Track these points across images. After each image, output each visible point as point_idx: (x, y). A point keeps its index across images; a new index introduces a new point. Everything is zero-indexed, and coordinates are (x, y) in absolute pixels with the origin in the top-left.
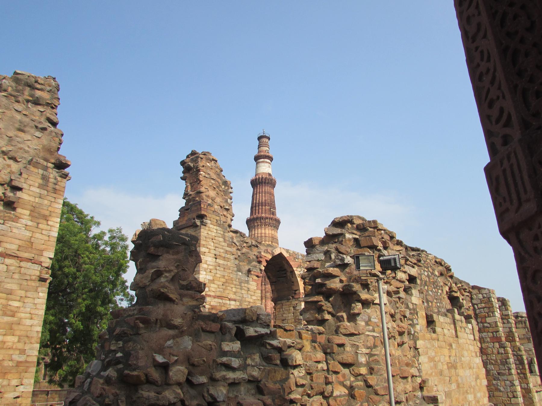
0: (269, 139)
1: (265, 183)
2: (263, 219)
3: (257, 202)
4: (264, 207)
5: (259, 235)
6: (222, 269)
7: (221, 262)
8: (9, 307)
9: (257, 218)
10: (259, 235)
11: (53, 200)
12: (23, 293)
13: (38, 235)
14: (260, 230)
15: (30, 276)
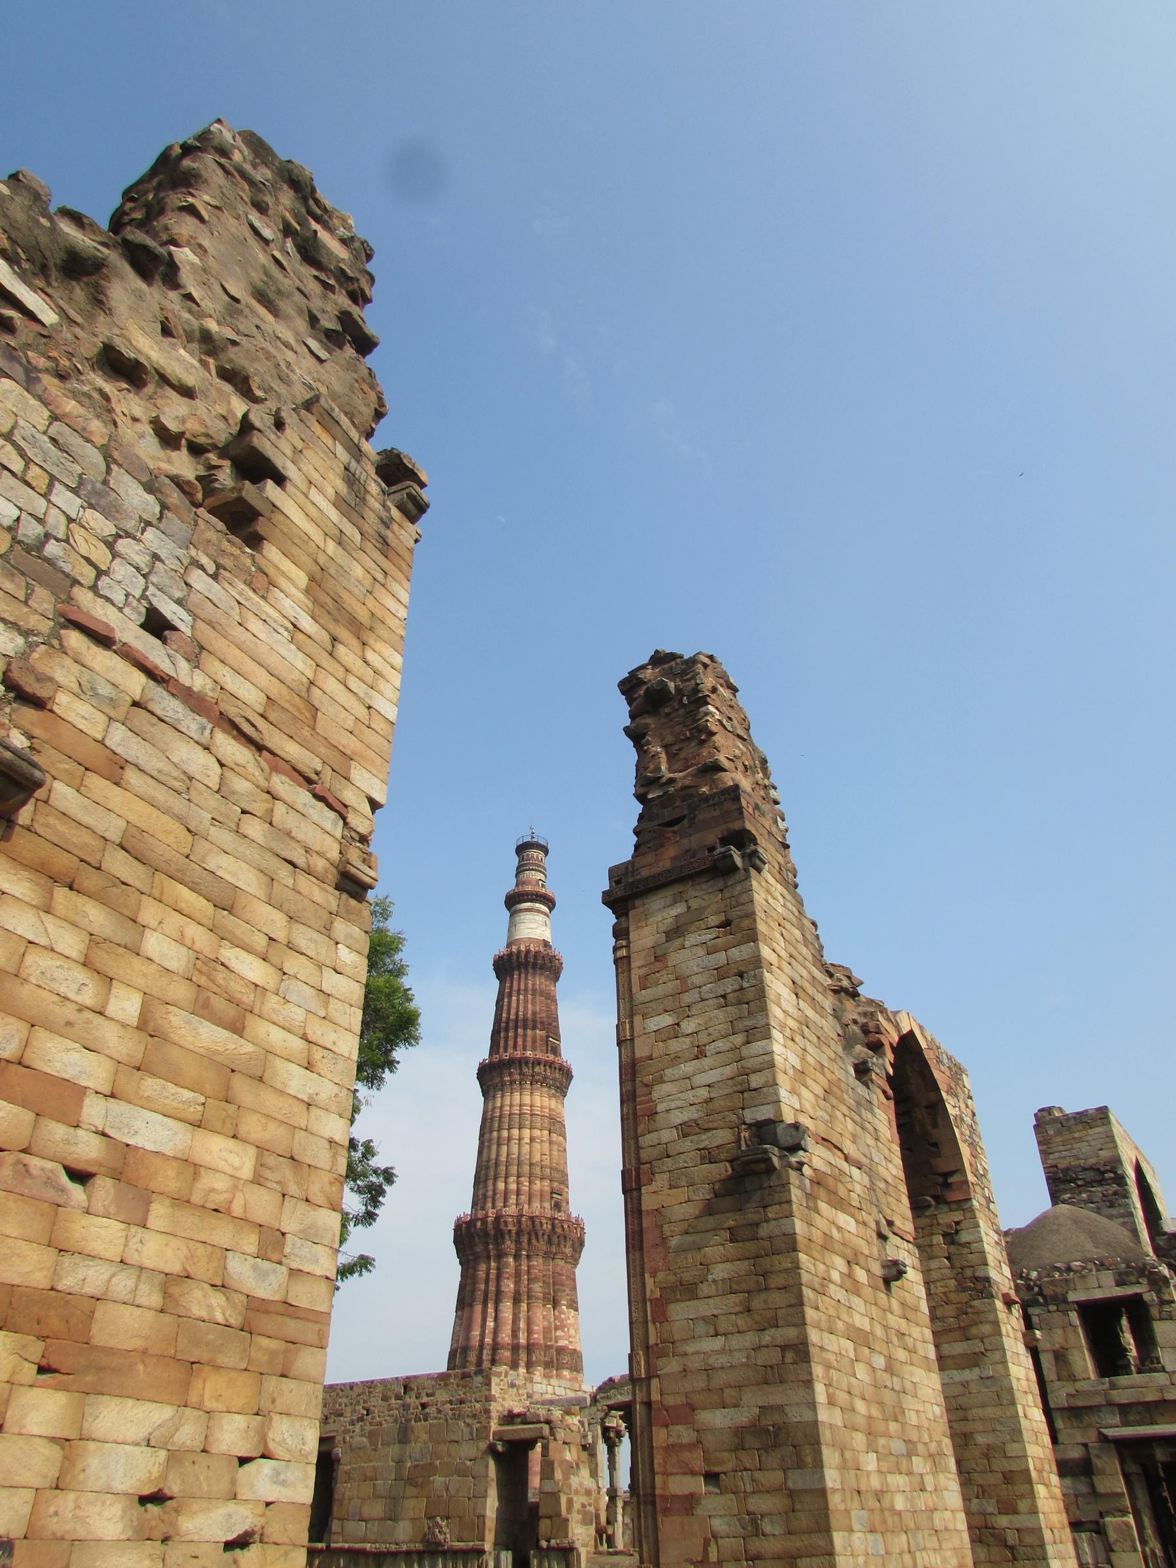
0: (545, 850)
1: (534, 966)
2: (527, 1063)
3: (513, 1017)
4: (529, 1032)
5: (516, 1110)
6: (815, 1040)
7: (810, 1013)
8: (221, 976)
9: (511, 1062)
10: (516, 1110)
11: (380, 577)
12: (276, 922)
13: (332, 685)
14: (517, 1096)
15: (307, 850)
